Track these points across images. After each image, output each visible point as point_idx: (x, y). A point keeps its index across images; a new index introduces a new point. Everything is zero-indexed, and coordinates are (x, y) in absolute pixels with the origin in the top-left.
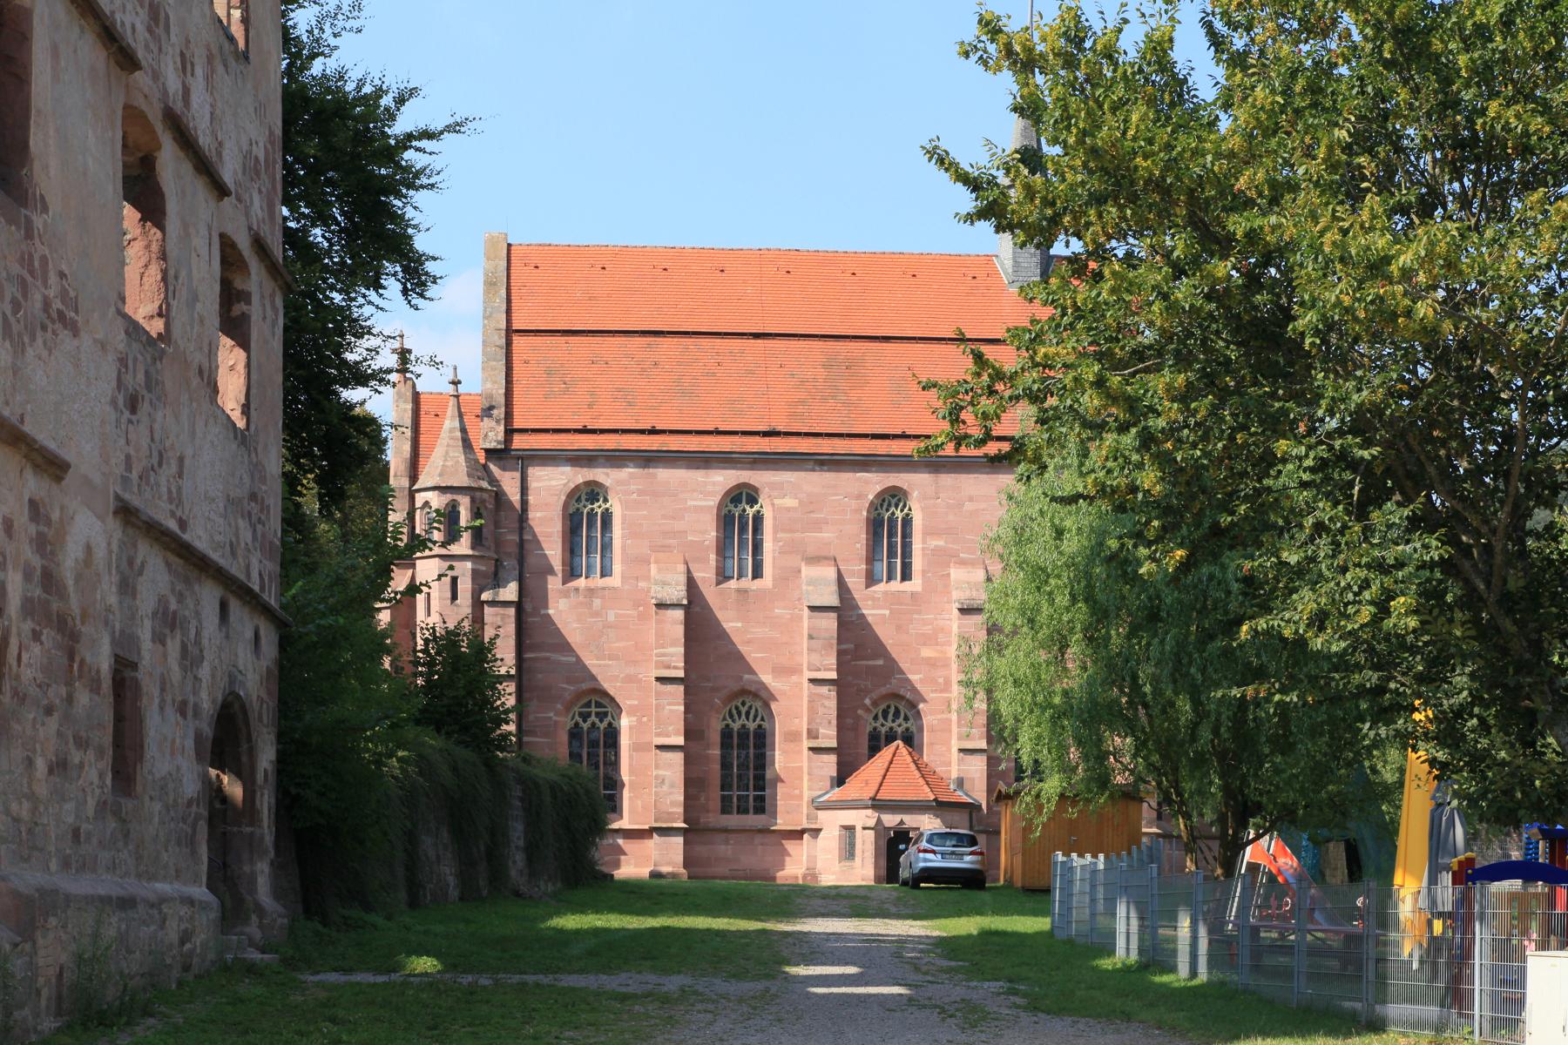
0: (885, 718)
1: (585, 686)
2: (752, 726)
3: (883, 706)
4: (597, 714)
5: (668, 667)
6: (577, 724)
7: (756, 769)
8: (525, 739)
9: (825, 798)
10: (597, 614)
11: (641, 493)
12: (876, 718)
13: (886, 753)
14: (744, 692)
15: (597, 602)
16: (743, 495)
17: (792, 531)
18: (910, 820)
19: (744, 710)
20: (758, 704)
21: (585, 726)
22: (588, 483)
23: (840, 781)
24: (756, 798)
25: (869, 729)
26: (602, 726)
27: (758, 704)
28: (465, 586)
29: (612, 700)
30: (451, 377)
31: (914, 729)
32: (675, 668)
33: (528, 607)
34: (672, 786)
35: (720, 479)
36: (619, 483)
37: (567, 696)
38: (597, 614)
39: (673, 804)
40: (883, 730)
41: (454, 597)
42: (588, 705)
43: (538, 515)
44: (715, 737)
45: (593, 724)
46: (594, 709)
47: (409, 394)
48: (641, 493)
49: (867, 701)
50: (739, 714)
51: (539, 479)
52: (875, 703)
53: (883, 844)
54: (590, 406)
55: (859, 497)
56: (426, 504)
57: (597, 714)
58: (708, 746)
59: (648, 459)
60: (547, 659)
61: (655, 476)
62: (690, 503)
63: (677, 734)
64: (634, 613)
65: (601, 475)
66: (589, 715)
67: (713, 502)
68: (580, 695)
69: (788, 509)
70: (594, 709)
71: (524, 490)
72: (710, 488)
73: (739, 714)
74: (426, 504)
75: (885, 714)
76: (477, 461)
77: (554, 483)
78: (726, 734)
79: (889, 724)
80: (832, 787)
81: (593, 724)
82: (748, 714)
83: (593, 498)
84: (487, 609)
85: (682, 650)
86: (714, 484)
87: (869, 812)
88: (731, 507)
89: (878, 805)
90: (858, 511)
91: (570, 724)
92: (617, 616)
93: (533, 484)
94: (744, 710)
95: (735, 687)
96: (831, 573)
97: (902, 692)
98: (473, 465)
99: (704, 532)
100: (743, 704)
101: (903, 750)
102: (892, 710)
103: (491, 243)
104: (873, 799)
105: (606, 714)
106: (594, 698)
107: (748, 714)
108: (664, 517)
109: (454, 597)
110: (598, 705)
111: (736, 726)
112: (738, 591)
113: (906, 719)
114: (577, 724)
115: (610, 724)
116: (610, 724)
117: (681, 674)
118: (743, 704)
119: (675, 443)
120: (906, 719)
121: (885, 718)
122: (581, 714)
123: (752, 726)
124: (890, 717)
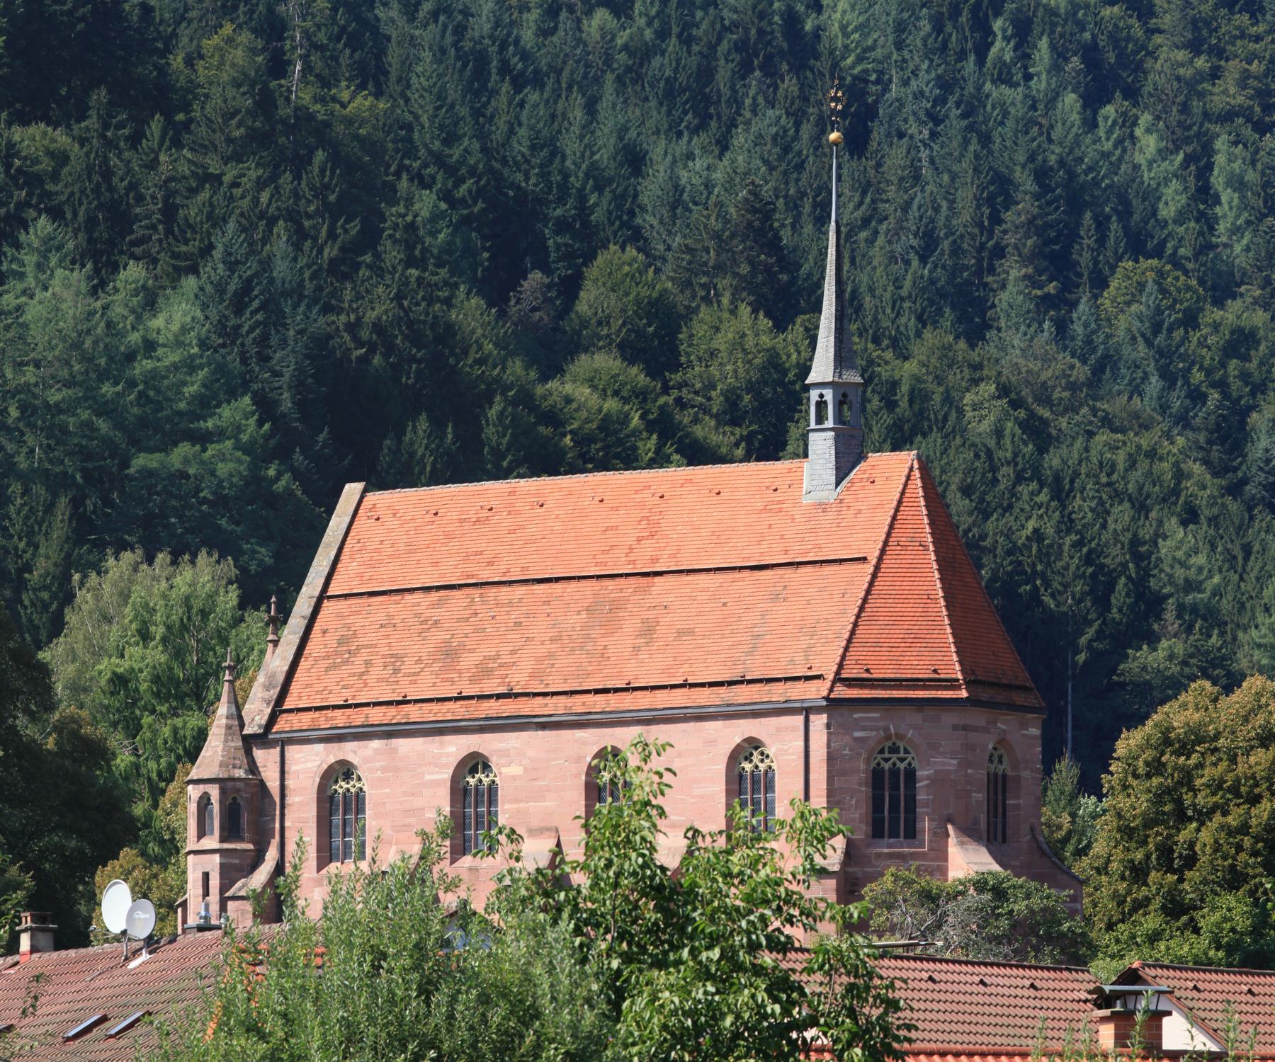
11: (385, 769)
16: (475, 763)
17: (517, 801)
28: (215, 882)
35: (452, 749)
43: (297, 799)
55: (579, 759)
61: (394, 750)
62: (428, 777)
65: (351, 751)
67: (447, 775)
69: (514, 778)
72: (444, 760)
86: (448, 755)
90: (577, 776)
93: (291, 767)
96: (551, 844)
109: (206, 893)
119: (415, 713)
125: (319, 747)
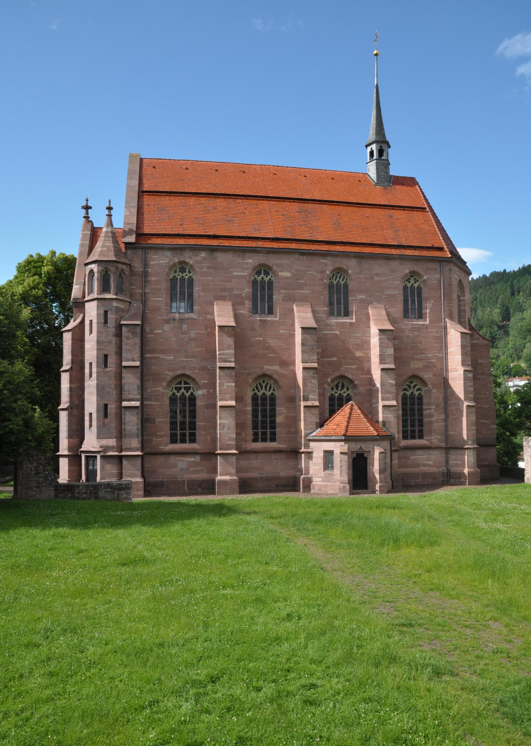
0: (337, 389)
1: (179, 372)
2: (268, 394)
3: (336, 382)
4: (185, 388)
5: (226, 361)
6: (174, 394)
7: (271, 417)
8: (145, 402)
9: (314, 434)
10: (185, 333)
11: (208, 268)
12: (332, 389)
13: (346, 409)
14: (264, 375)
15: (185, 327)
18: (365, 446)
19: (264, 385)
20: (272, 382)
21: (178, 395)
22: (180, 263)
23: (321, 425)
24: (271, 433)
25: (329, 394)
26: (188, 395)
27: (272, 382)
29: (194, 380)
30: (107, 205)
31: (352, 394)
32: (230, 362)
33: (147, 329)
34: (229, 429)
36: (198, 262)
37: (169, 378)
38: (185, 333)
39: (230, 439)
40: (337, 395)
41: (106, 322)
42: (180, 383)
44: (249, 400)
45: (183, 394)
46: (183, 385)
47: (90, 227)
48: (208, 268)
49: (329, 380)
50: (261, 387)
51: (154, 260)
52: (332, 381)
53: (351, 461)
54: (181, 225)
56: (92, 271)
57: (185, 388)
58: (246, 405)
59: (212, 249)
60: (158, 358)
62: (235, 274)
63: (231, 399)
64: (205, 332)
66: (181, 388)
68: (176, 377)
70: (183, 385)
71: (146, 265)
72: (245, 266)
73: (261, 387)
74: (92, 271)
75: (337, 386)
76: (120, 249)
77: (162, 262)
78: (255, 398)
79: (339, 392)
80: (317, 428)
81: (183, 394)
82: (266, 387)
83: (183, 270)
84: (124, 329)
85: (233, 351)
86: (247, 264)
87: (343, 443)
88: (256, 276)
89: (347, 439)
91: (170, 393)
92: (196, 334)
94: (264, 385)
95: (260, 373)
97: (347, 375)
98: (117, 251)
99: (242, 289)
100: (264, 382)
101: (356, 407)
102: (340, 384)
103: (131, 156)
104: (344, 435)
105: (190, 388)
106: (183, 379)
107: (266, 387)
108: (221, 281)
110: (186, 383)
111: (260, 394)
112: (261, 320)
113: (348, 389)
114: (174, 394)
115: (192, 394)
116: (192, 394)
117: (232, 365)
118: (264, 382)
119: (226, 243)
120: (348, 389)
121: (337, 389)
122: (176, 388)
123: (268, 394)
124: (340, 388)
125: (169, 253)
